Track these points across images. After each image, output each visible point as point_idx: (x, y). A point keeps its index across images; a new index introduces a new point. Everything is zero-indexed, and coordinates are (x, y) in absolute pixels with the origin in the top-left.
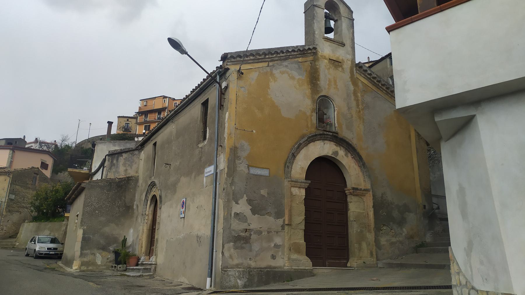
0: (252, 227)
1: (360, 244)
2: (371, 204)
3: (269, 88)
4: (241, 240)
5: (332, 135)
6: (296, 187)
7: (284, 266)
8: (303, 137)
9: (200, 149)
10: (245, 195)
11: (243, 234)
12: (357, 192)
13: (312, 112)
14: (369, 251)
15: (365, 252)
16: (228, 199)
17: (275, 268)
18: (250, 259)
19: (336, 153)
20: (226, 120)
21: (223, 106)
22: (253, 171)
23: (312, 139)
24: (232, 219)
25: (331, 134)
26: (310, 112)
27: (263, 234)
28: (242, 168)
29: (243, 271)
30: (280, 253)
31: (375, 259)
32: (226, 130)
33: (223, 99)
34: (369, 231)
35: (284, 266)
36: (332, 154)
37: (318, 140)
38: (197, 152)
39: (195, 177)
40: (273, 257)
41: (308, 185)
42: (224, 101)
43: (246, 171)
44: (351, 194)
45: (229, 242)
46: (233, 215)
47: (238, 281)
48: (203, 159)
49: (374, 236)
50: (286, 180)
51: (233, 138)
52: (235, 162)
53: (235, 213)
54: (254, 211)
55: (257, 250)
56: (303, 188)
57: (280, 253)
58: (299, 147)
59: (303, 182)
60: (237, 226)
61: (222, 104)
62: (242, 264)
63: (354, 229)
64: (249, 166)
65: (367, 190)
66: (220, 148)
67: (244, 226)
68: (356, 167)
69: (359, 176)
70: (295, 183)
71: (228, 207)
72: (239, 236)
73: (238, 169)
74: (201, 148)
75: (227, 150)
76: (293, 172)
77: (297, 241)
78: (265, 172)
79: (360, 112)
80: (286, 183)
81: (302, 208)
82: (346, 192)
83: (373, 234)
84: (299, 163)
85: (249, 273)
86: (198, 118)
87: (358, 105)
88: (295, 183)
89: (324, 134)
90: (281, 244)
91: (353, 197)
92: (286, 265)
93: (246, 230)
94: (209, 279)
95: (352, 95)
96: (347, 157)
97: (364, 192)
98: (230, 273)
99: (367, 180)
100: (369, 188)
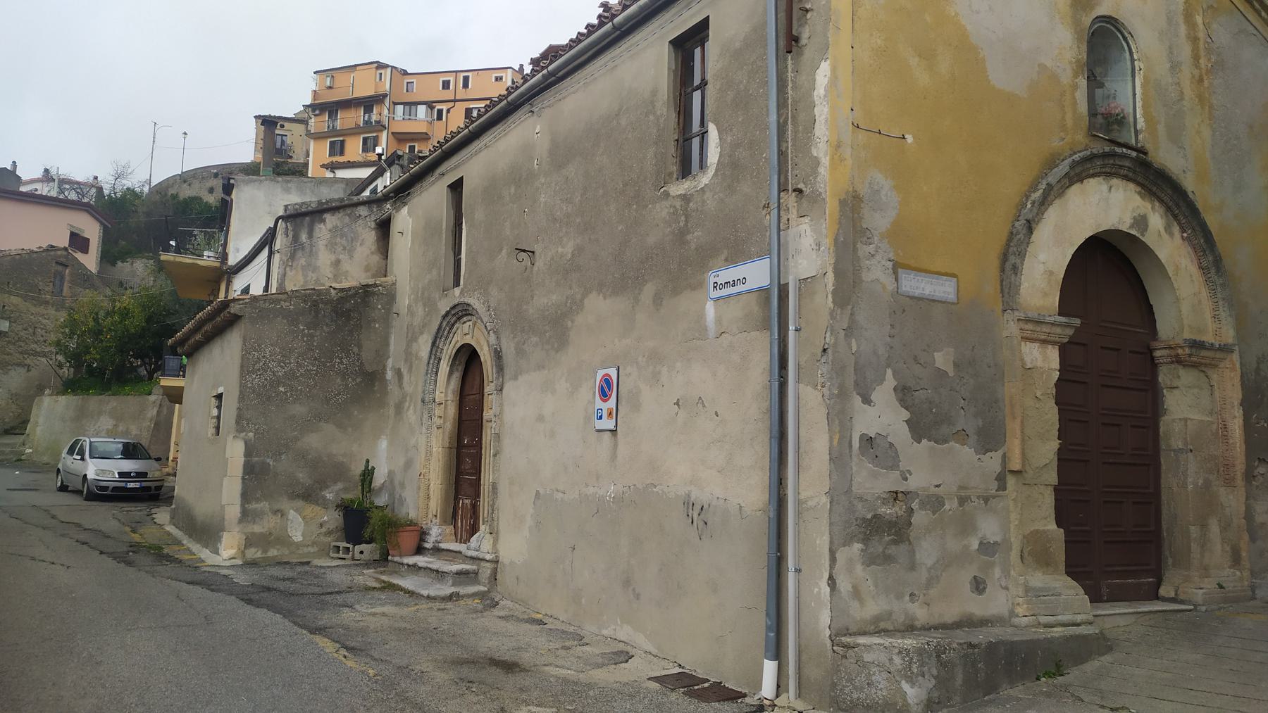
0: (913, 484)
1: (1204, 526)
4: (882, 531)
7: (1012, 614)
8: (1051, 163)
9: (678, 204)
10: (889, 372)
11: (887, 511)
12: (1198, 355)
13: (1076, 76)
15: (1218, 551)
16: (842, 388)
17: (984, 622)
18: (912, 595)
19: (1141, 222)
20: (820, 91)
21: (797, 40)
22: (915, 285)
23: (1080, 171)
24: (855, 459)
25: (1134, 154)
26: (1069, 72)
27: (947, 507)
28: (876, 272)
29: (920, 651)
30: (997, 572)
31: (1246, 574)
32: (821, 130)
33: (796, 13)
34: (1229, 482)
35: (1012, 614)
36: (1132, 227)
37: (1093, 176)
38: (661, 211)
39: (658, 300)
40: (979, 586)
41: (1070, 332)
42: (803, 22)
43: (891, 285)
44: (1178, 360)
45: (847, 542)
46: (856, 444)
47: (905, 686)
48: (697, 237)
50: (1009, 316)
51: (849, 162)
52: (855, 250)
53: (863, 436)
54: (919, 429)
55: (930, 562)
56: (1054, 343)
57: (997, 572)
59: (1060, 325)
60: (871, 483)
61: (794, 33)
62: (890, 614)
63: (1183, 479)
64: (897, 267)
65: (1225, 349)
66: (790, 199)
67: (888, 482)
68: (1193, 269)
69: (1200, 301)
70: (1033, 326)
71: (839, 418)
72: (875, 516)
73: (867, 277)
74: (685, 198)
75: (831, 206)
76: (1025, 287)
78: (944, 289)
80: (1010, 327)
81: (1051, 413)
82: (1157, 354)
83: (1242, 492)
84: (1042, 257)
85: (938, 656)
86: (654, 93)
87: (1196, 58)
88: (1033, 326)
90: (998, 539)
91: (1182, 372)
92: (1019, 611)
93: (895, 496)
94: (770, 667)
95: (1181, 20)
96: (1171, 234)
97: (1219, 355)
98: (868, 657)
99: (1223, 315)
100: (1230, 341)
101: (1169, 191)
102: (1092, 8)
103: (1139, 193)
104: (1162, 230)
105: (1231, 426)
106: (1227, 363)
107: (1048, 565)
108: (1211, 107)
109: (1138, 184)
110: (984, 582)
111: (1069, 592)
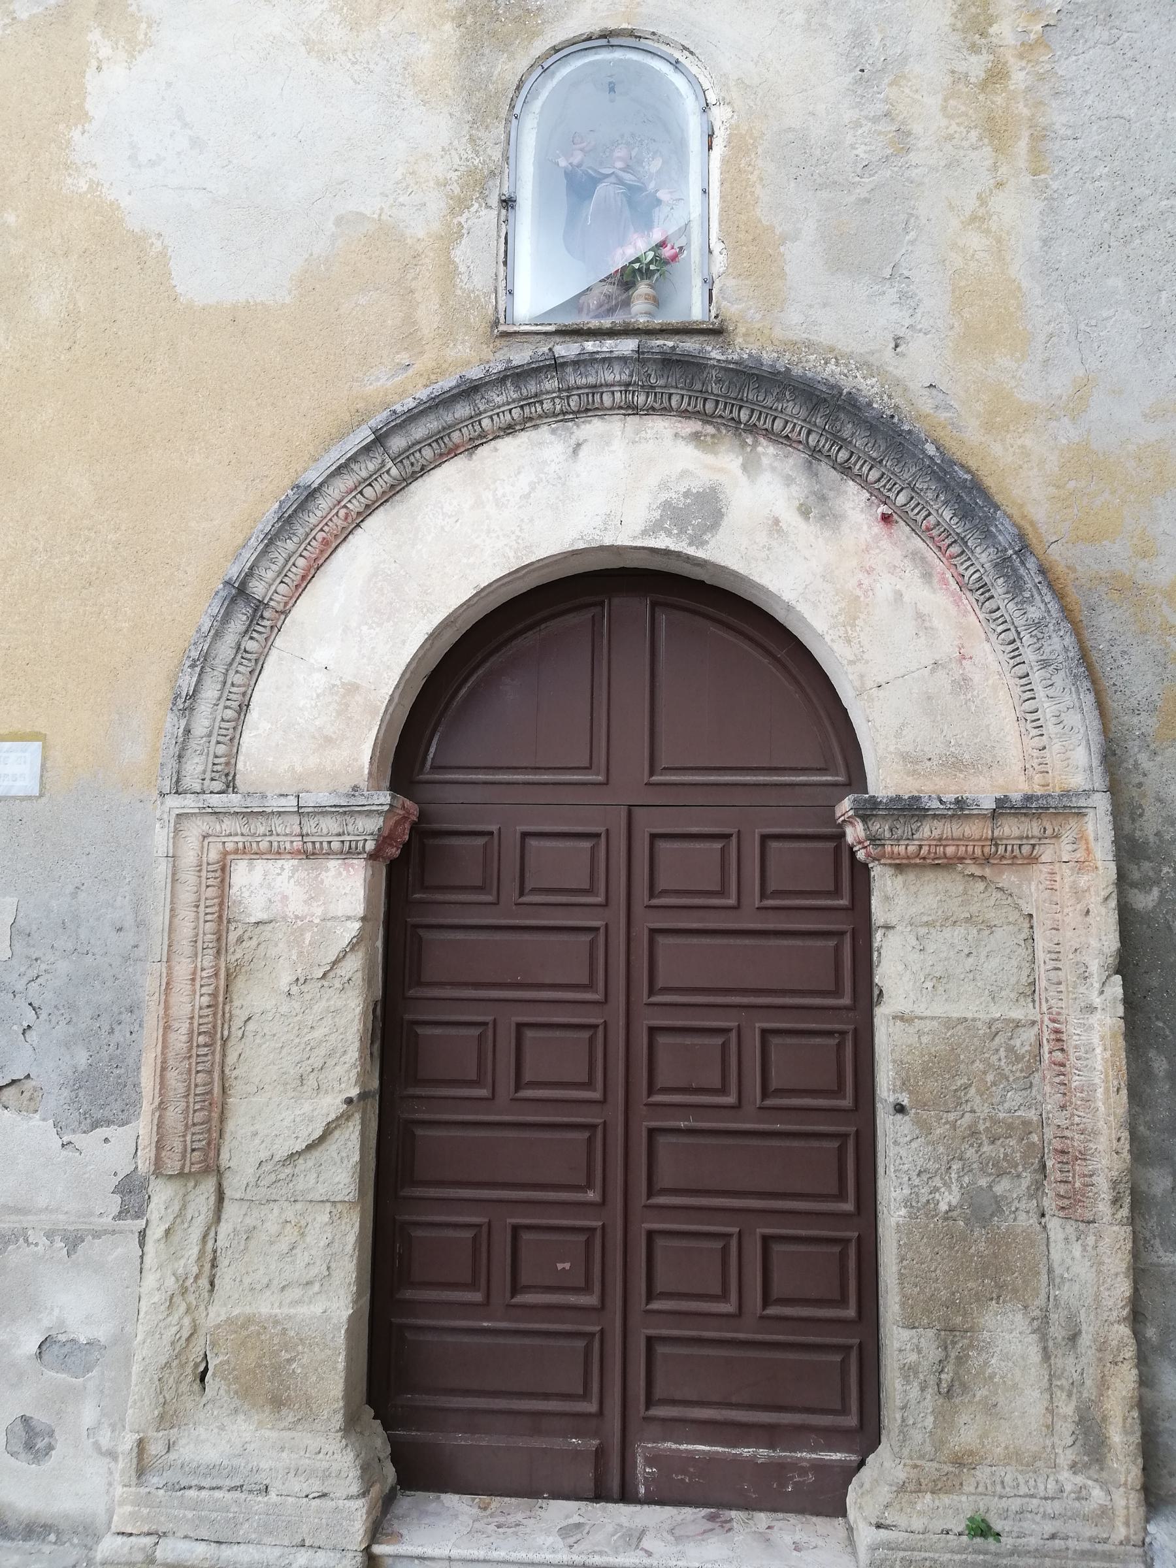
2: (1103, 938)
3: (84, 117)
5: (640, 358)
6: (278, 854)
13: (460, 204)
14: (1067, 1408)
25: (627, 346)
26: (436, 204)
30: (89, 1414)
34: (1073, 1204)
36: (655, 528)
49: (1117, 1262)
56: (349, 852)
57: (89, 1414)
58: (305, 528)
65: (1044, 809)
69: (963, 684)
77: (265, 1307)
79: (996, 75)
84: (322, 655)
89: (557, 366)
90: (101, 1333)
97: (1010, 828)
99: (1048, 710)
100: (1078, 781)
101: (791, 408)
102: (534, 34)
103: (696, 437)
104: (790, 518)
105: (1075, 1035)
106: (1065, 849)
107: (277, 1403)
108: (1040, 137)
109: (685, 414)
110: (51, 1434)
111: (297, 1485)
